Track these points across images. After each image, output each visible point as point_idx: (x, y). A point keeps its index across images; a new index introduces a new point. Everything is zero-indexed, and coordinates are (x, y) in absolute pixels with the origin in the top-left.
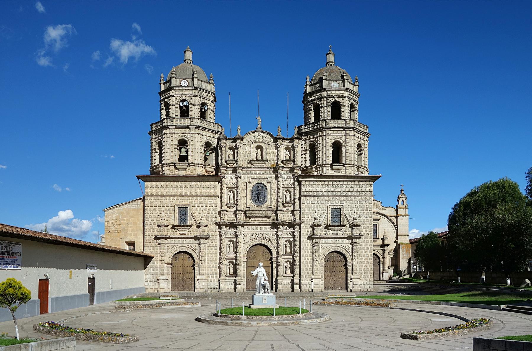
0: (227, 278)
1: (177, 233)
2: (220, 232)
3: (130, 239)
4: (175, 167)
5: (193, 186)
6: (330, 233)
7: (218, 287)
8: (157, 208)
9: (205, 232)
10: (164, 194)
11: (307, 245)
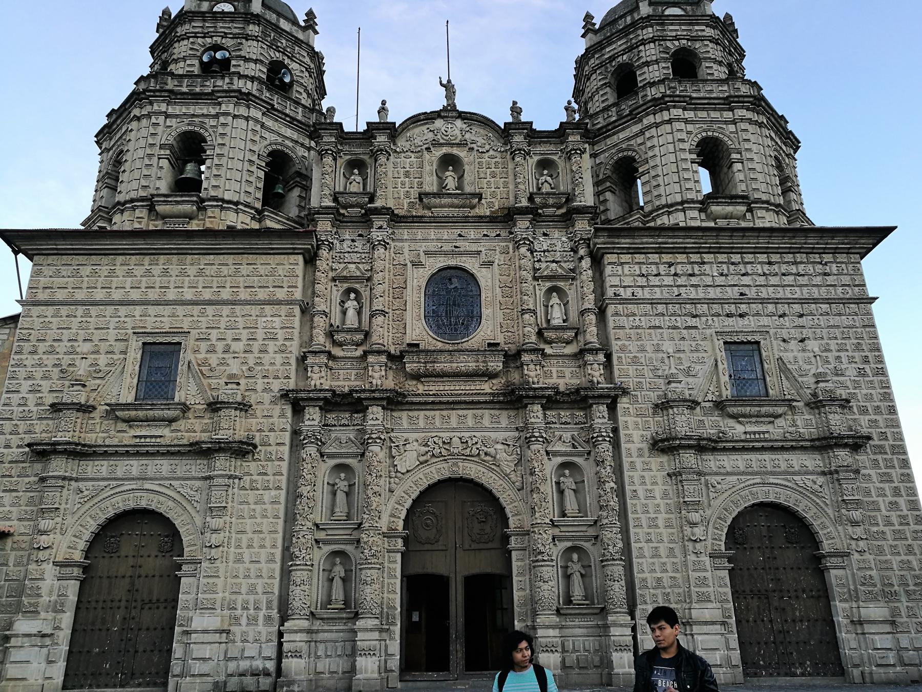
0: (317, 625)
1: (127, 436)
2: (296, 433)
4: (151, 209)
5: (210, 270)
6: (737, 430)
7: (271, 666)
8: (61, 347)
9: (233, 427)
10: (99, 295)
11: (647, 477)
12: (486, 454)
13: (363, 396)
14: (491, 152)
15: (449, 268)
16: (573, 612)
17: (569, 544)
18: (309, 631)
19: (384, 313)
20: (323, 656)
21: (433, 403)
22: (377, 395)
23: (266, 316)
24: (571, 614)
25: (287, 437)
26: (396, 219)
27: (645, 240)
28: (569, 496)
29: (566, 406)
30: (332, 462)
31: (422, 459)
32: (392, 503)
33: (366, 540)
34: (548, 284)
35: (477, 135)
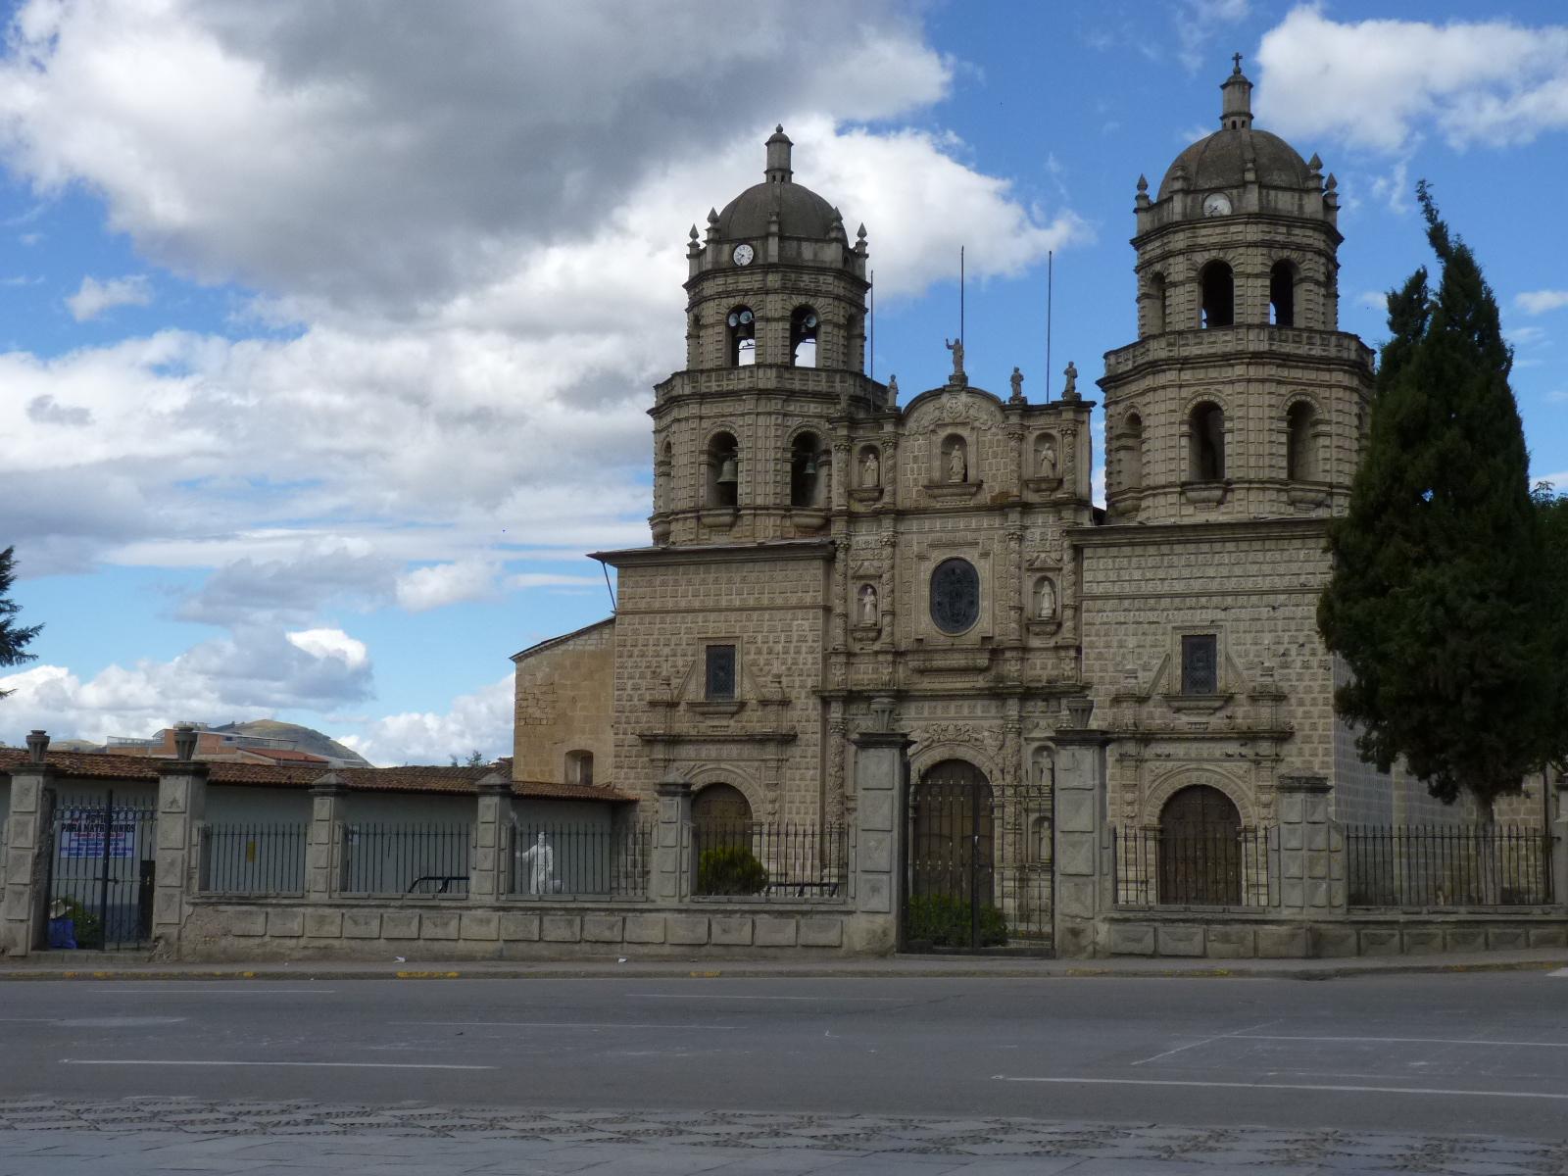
1: (706, 726)
3: (580, 742)
34: (1039, 575)
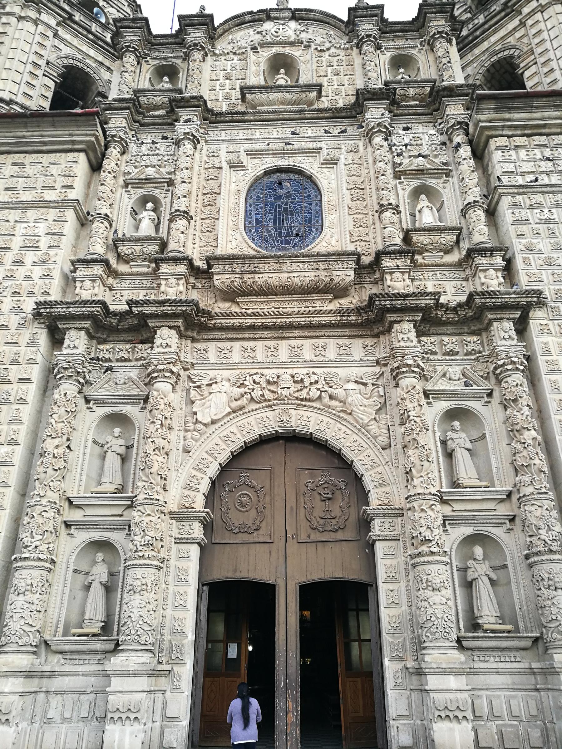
0: (54, 662)
12: (331, 397)
13: (147, 310)
14: (333, 50)
15: (279, 170)
16: (485, 644)
17: (468, 531)
18: (29, 675)
19: (187, 215)
20: (58, 719)
21: (252, 327)
22: (167, 309)
23: (28, 221)
24: (480, 649)
25: (35, 373)
26: (212, 117)
27: (546, 114)
28: (463, 459)
29: (450, 329)
30: (101, 411)
31: (235, 404)
32: (187, 470)
33: (137, 520)
34: (414, 183)
35: (316, 34)
